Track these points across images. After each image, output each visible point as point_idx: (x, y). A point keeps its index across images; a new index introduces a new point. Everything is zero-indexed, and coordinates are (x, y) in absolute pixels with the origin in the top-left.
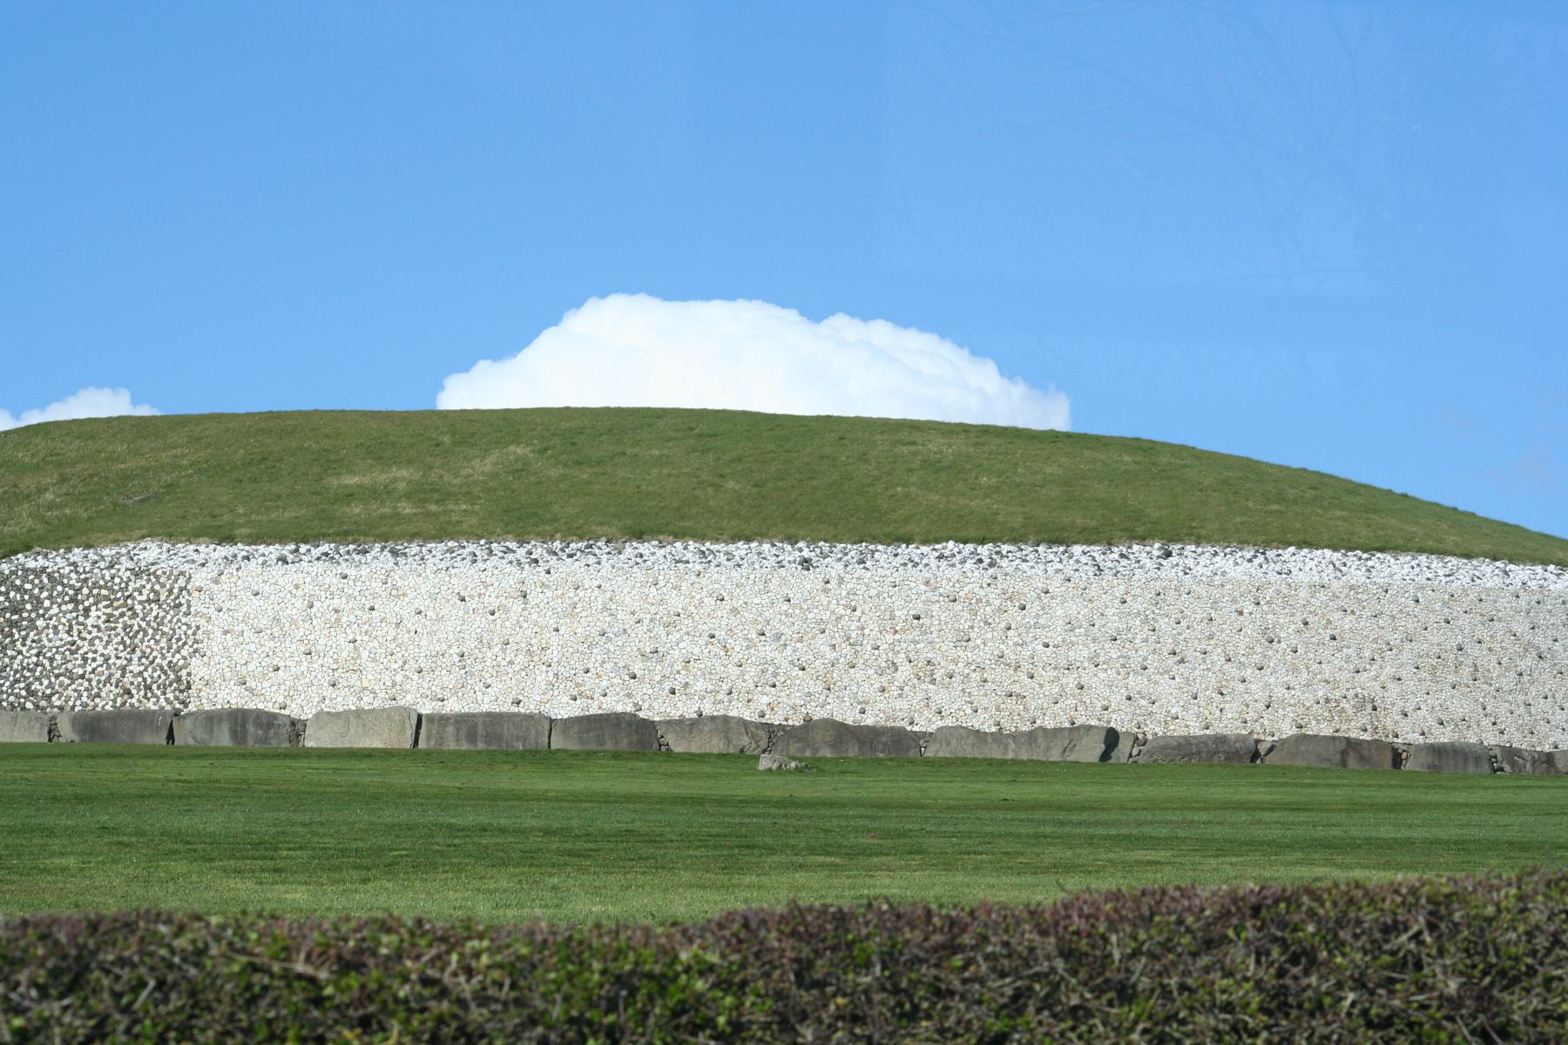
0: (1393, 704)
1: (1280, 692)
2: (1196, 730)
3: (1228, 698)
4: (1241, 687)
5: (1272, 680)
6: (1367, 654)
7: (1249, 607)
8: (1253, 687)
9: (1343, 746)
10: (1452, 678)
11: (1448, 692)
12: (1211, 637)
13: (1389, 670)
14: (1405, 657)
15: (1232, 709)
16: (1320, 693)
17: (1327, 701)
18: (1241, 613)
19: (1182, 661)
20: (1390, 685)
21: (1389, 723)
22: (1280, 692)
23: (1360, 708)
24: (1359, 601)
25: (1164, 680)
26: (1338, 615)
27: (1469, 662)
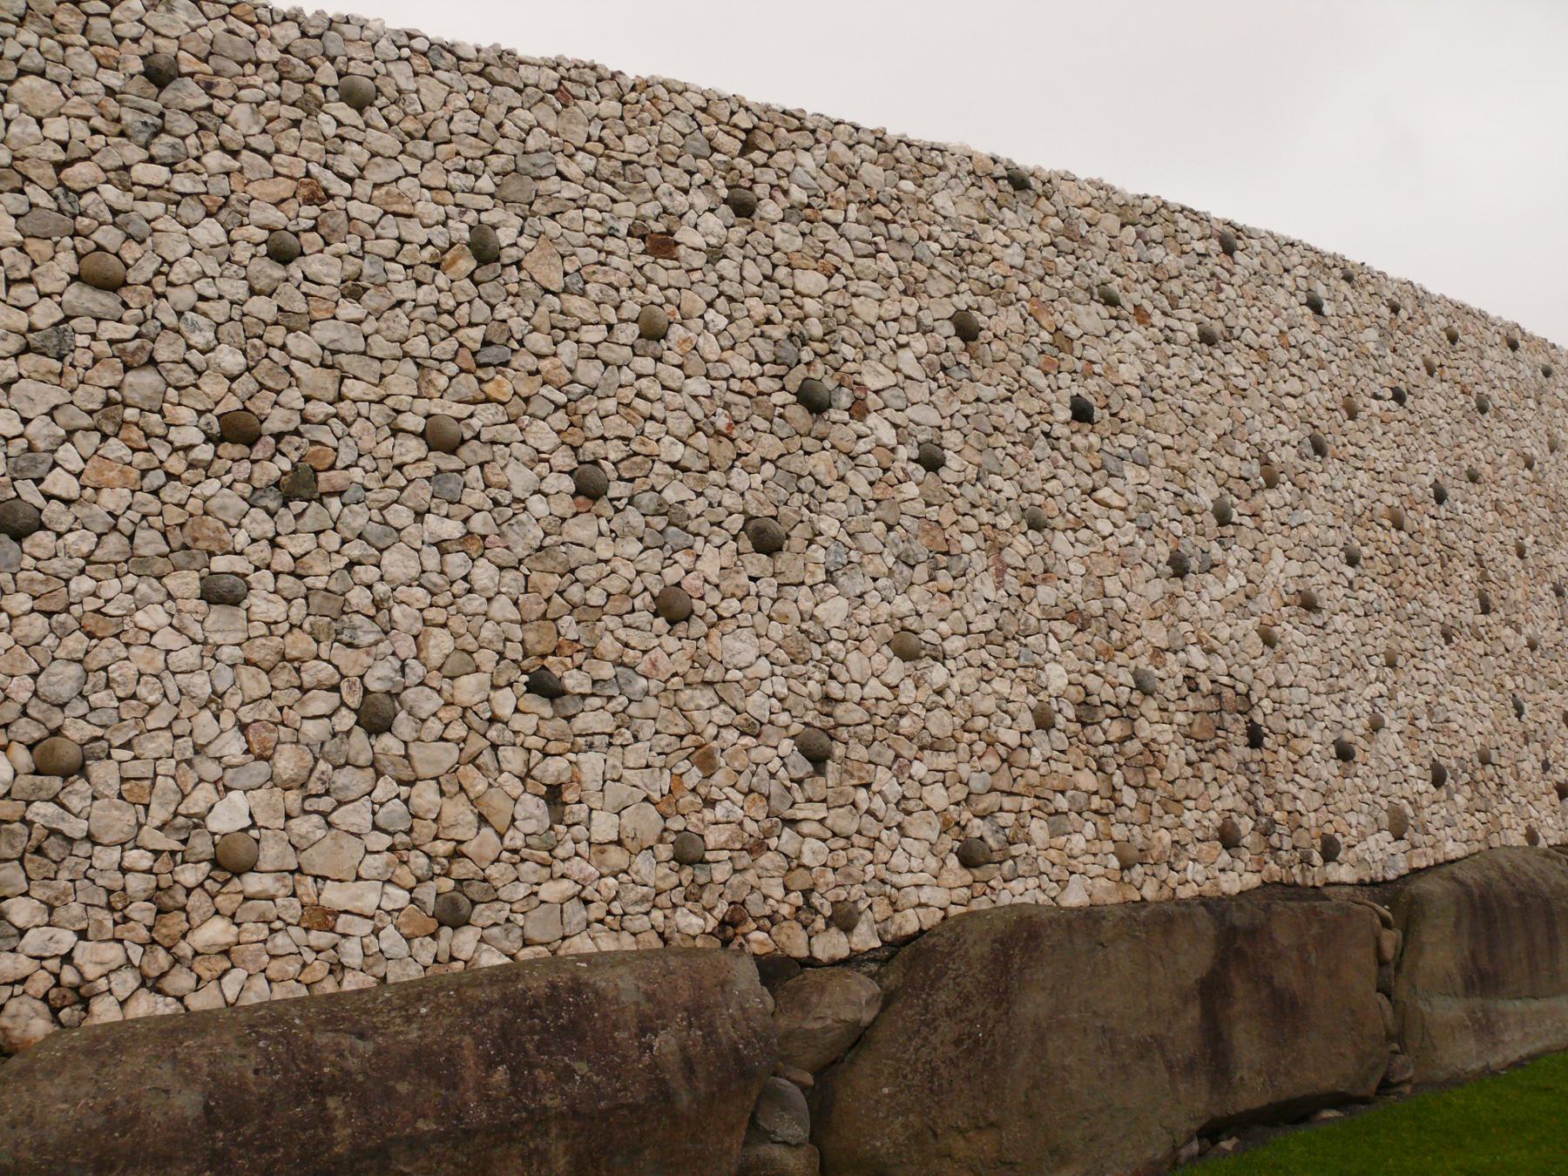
0: (1309, 714)
1: (871, 671)
2: (378, 938)
3: (593, 719)
4: (670, 650)
5: (834, 610)
6: (1206, 496)
7: (705, 226)
8: (739, 648)
9: (1194, 957)
10: (1439, 607)
11: (1441, 659)
12: (488, 357)
13: (1281, 570)
14: (1317, 517)
15: (618, 789)
16: (1056, 677)
17: (1087, 712)
18: (662, 246)
19: (299, 487)
20: (1292, 634)
21: (1307, 800)
22: (871, 671)
23: (1203, 743)
24: (1160, 278)
25: (161, 613)
26: (1092, 316)
27: (1465, 548)
